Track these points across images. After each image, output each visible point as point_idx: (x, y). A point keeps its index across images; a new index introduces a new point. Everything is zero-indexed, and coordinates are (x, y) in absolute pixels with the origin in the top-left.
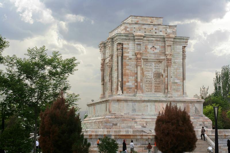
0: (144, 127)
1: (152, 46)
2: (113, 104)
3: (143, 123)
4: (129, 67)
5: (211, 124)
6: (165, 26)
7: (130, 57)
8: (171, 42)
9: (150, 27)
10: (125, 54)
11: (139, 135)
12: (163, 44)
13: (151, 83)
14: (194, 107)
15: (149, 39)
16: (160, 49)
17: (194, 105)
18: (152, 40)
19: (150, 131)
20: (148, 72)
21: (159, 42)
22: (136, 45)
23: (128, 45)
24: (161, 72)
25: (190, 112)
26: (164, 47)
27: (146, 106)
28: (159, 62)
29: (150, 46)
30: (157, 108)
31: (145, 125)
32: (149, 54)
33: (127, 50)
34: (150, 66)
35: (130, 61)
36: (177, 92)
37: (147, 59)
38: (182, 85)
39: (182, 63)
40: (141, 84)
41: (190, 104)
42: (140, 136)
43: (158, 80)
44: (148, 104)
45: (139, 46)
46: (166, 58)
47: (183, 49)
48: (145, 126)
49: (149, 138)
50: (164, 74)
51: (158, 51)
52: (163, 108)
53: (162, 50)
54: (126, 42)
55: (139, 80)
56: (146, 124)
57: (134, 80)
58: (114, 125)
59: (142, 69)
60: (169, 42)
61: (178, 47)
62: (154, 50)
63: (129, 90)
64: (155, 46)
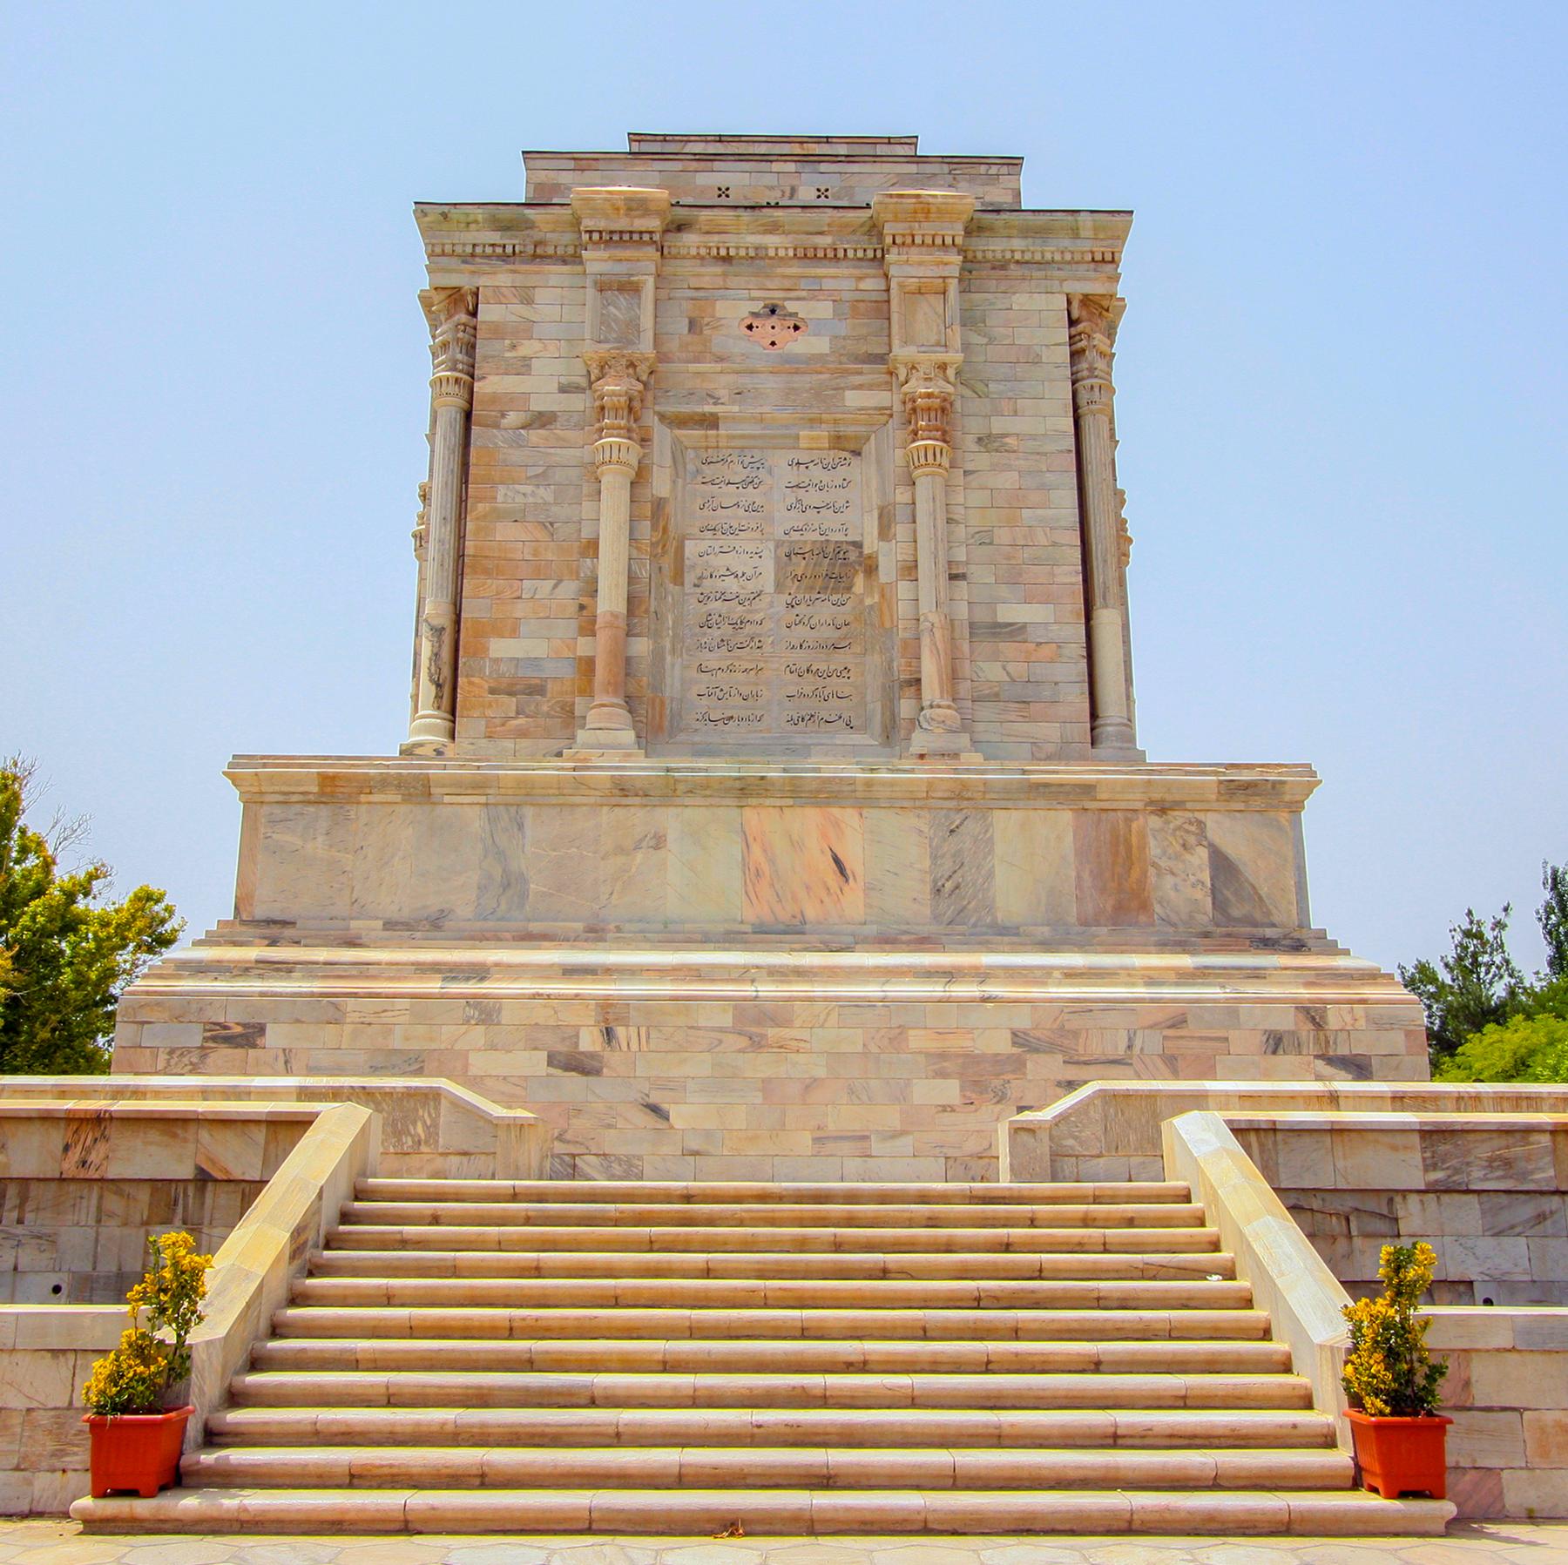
0: (585, 1071)
1: (758, 307)
2: (273, 822)
3: (569, 1018)
4: (528, 489)
5: (1408, 1034)
6: (913, 168)
7: (537, 406)
8: (940, 255)
9: (770, 180)
10: (491, 378)
11: (47, 1118)
12: (868, 284)
13: (756, 642)
14: (1203, 854)
15: (731, 240)
16: (843, 328)
17: (1201, 824)
18: (758, 256)
19: (655, 1109)
20: (727, 542)
21: (832, 271)
22: (591, 292)
23: (529, 301)
25: (1158, 908)
26: (881, 309)
27: (637, 848)
28: (837, 442)
29: (734, 309)
30: (772, 861)
32: (731, 378)
33: (514, 347)
34: (749, 482)
35: (535, 436)
36: (1027, 719)
37: (711, 422)
39: (1070, 443)
40: (641, 646)
41: (1155, 821)
42: (57, 1137)
43: (824, 611)
44: (670, 820)
45: (622, 300)
46: (897, 398)
47: (1072, 323)
48: (592, 1056)
49: (203, 1179)
51: (821, 345)
52: (837, 860)
53: (865, 338)
56: (609, 1034)
57: (572, 609)
58: (221, 1036)
59: (650, 512)
60: (915, 255)
61: (1020, 300)
62: (782, 334)
63: (511, 703)
64: (791, 307)
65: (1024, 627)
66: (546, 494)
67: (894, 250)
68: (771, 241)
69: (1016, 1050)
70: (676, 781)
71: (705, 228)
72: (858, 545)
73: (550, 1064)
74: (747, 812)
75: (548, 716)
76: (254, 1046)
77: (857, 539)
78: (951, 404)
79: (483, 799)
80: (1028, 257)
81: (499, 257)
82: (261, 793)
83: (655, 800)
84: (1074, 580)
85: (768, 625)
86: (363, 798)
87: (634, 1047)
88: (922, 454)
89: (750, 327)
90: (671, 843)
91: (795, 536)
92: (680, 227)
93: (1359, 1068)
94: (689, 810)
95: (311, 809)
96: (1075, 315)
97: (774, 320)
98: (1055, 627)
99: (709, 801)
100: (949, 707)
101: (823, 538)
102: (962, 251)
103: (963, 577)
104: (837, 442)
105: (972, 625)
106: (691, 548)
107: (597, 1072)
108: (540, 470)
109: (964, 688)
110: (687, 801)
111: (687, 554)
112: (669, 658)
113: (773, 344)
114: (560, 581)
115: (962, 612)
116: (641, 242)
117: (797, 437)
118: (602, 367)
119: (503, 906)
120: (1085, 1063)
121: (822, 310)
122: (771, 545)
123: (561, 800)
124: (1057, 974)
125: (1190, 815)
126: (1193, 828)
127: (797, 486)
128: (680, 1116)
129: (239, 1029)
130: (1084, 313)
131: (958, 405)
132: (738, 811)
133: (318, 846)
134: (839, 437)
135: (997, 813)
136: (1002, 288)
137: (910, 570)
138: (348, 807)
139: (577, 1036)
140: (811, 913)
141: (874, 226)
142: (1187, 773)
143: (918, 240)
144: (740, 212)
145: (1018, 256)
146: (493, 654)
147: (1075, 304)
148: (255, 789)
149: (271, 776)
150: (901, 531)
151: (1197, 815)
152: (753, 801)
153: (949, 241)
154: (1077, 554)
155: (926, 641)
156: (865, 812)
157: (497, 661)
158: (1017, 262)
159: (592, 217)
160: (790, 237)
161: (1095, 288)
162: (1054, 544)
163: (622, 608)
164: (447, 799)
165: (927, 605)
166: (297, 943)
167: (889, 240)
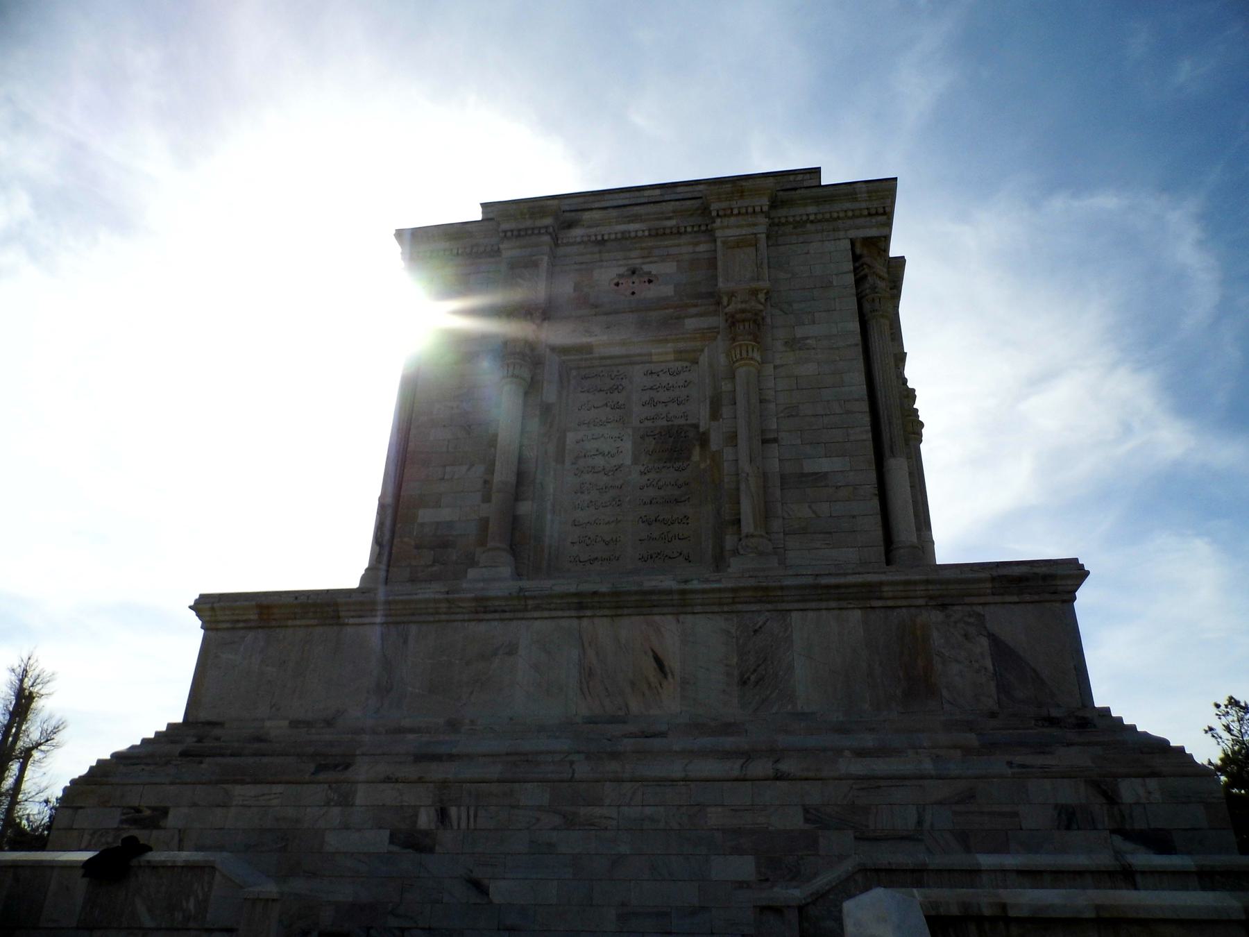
1: (622, 270)
8: (751, 219)
14: (984, 642)
17: (980, 617)
19: (478, 886)
25: (945, 693)
26: (712, 263)
31: (425, 820)
34: (611, 390)
38: (870, 487)
41: (936, 616)
47: (856, 258)
48: (427, 833)
51: (668, 290)
56: (443, 815)
64: (646, 268)
65: (825, 475)
67: (718, 220)
69: (807, 827)
72: (696, 426)
73: (391, 842)
74: (585, 622)
76: (158, 827)
77: (694, 422)
78: (763, 319)
80: (820, 216)
84: (864, 437)
87: (463, 825)
89: (617, 284)
91: (649, 423)
92: (570, 225)
93: (1159, 841)
94: (537, 623)
96: (858, 251)
97: (634, 278)
99: (554, 614)
100: (762, 536)
102: (768, 216)
103: (775, 440)
105: (783, 477)
106: (571, 437)
107: (431, 850)
109: (776, 525)
110: (536, 614)
111: (568, 441)
112: (549, 517)
113: (633, 293)
114: (472, 465)
115: (774, 465)
116: (539, 233)
120: (876, 839)
121: (669, 268)
122: (630, 431)
123: (437, 617)
124: (847, 753)
125: (968, 608)
126: (972, 620)
127: (651, 389)
128: (500, 891)
129: (148, 813)
130: (865, 252)
131: (769, 320)
132: (575, 622)
135: (794, 614)
136: (801, 240)
137: (732, 439)
139: (417, 816)
140: (635, 706)
143: (735, 211)
144: (610, 210)
145: (812, 217)
146: (420, 520)
147: (858, 245)
150: (726, 411)
151: (975, 608)
152: (589, 613)
153: (758, 209)
154: (866, 419)
155: (743, 486)
156: (681, 617)
157: (422, 525)
158: (812, 222)
161: (873, 232)
163: (512, 479)
164: (351, 621)
165: (745, 465)
167: (714, 214)
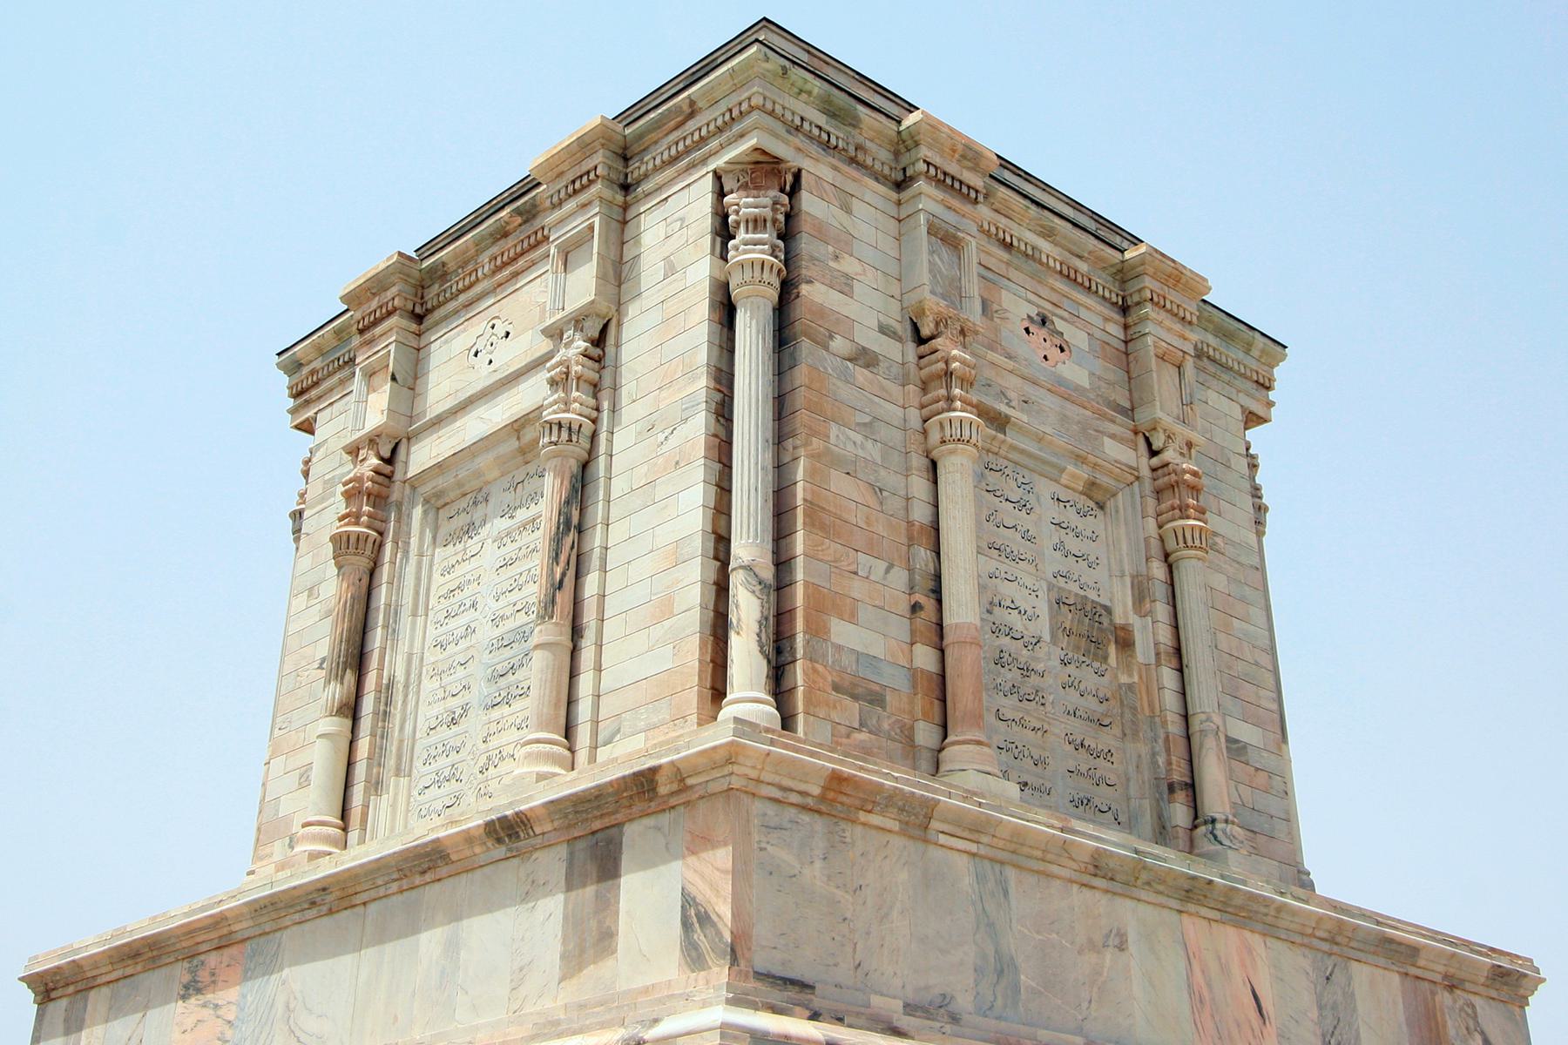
18: (1031, 256)
24: (1104, 601)
29: (1017, 306)
34: (1023, 506)
44: (1132, 914)
50: (1134, 620)
54: (825, 172)
55: (962, 608)
57: (904, 607)
64: (1060, 325)
66: (873, 451)
67: (1149, 305)
68: (1045, 245)
70: (1145, 867)
71: (997, 206)
75: (890, 738)
79: (973, 848)
81: (820, 143)
82: (758, 781)
83: (1117, 887)
85: (1049, 680)
86: (862, 816)
88: (1197, 535)
90: (1132, 947)
94: (1141, 906)
95: (806, 818)
98: (1265, 754)
101: (1082, 593)
104: (1091, 488)
108: (867, 419)
110: (1144, 895)
117: (1063, 470)
118: (937, 324)
119: (999, 1002)
123: (1041, 866)
132: (1175, 917)
133: (814, 874)
134: (1093, 484)
138: (843, 825)
141: (1120, 271)
142: (1472, 951)
148: (753, 774)
149: (782, 760)
159: (930, 147)
160: (1058, 250)
162: (1257, 664)
164: (942, 839)
166: (840, 1020)
